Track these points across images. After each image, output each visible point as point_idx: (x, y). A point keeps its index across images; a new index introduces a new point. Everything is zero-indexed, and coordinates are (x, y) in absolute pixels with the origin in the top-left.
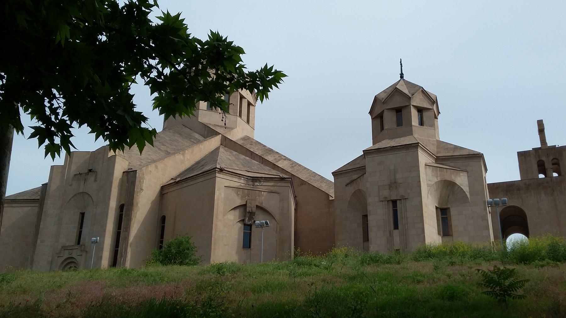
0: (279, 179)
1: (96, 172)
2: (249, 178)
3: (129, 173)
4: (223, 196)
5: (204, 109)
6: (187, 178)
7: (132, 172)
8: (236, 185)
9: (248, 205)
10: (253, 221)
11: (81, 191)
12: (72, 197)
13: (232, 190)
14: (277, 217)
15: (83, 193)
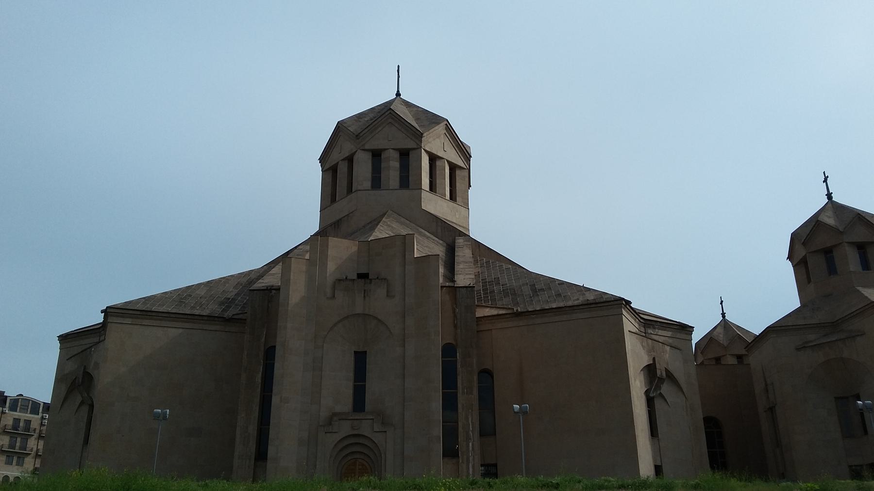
0: (678, 327)
1: (387, 281)
2: (642, 321)
3: (458, 289)
4: (630, 347)
5: (426, 190)
6: (543, 311)
7: (465, 289)
8: (634, 330)
9: (658, 366)
10: (659, 392)
11: (359, 310)
12: (339, 321)
13: (637, 338)
14: (685, 390)
15: (365, 316)
